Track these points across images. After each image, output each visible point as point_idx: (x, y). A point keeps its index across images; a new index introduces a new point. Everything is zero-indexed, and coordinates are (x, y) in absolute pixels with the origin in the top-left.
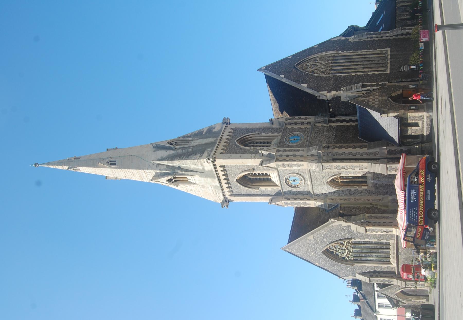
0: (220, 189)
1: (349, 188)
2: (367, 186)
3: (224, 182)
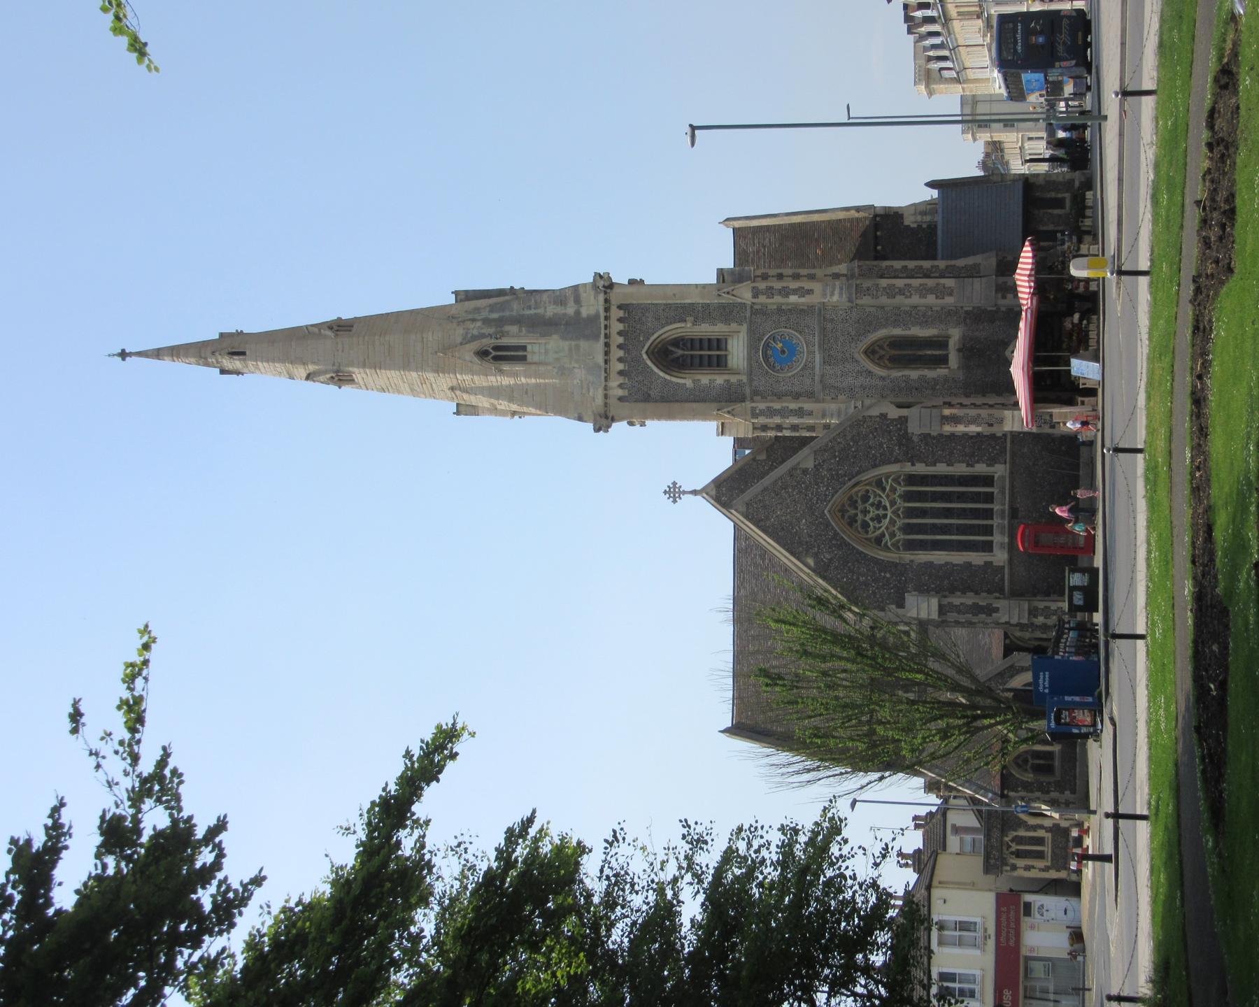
0: (603, 374)
1: (906, 372)
2: (949, 368)
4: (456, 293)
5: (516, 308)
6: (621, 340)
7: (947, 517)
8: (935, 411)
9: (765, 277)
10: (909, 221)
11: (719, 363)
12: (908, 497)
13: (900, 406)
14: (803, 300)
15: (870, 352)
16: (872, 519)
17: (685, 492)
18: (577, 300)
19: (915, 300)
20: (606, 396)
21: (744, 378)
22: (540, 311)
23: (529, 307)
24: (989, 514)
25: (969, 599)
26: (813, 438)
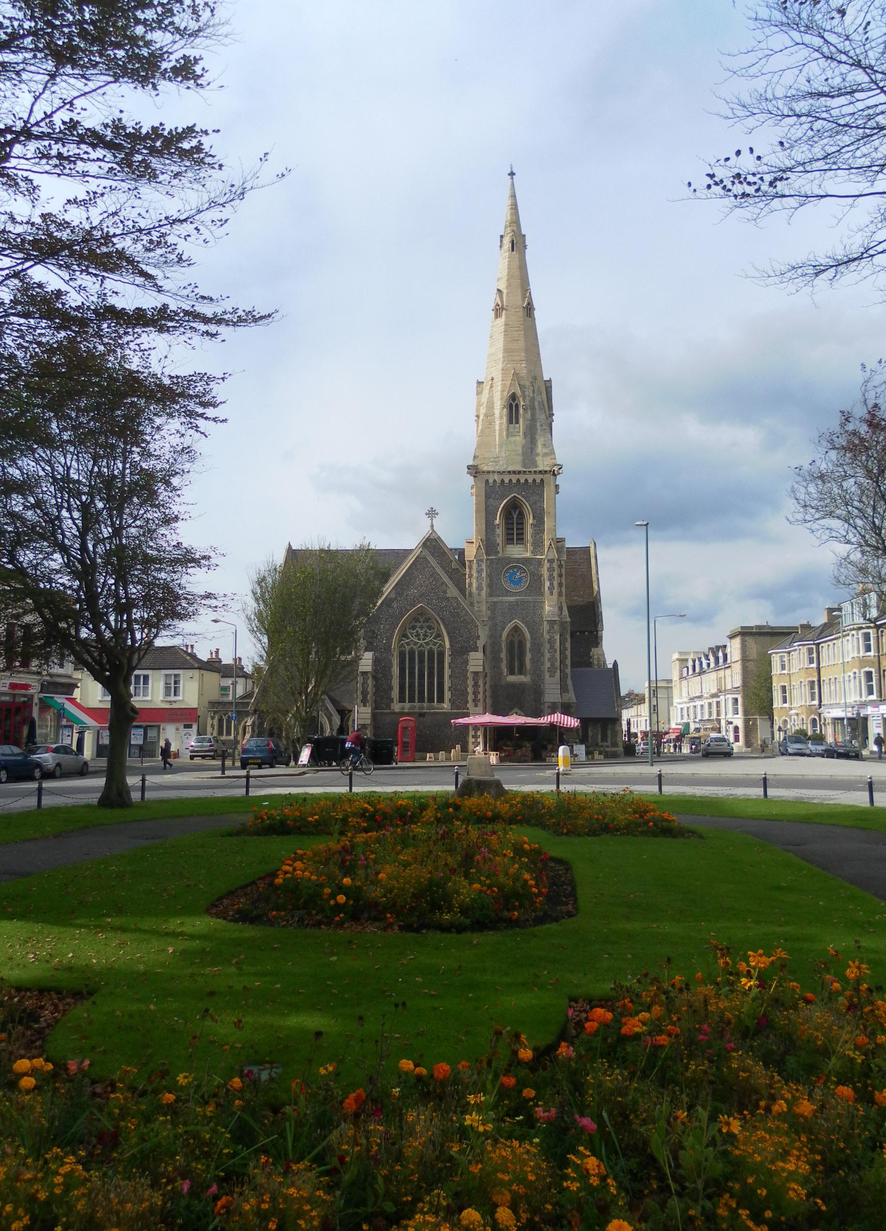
1: (504, 650)
3: (514, 478)
4: (550, 381)
5: (541, 417)
6: (522, 481)
7: (419, 676)
8: (480, 669)
9: (560, 566)
10: (594, 651)
11: (509, 540)
12: (431, 653)
13: (484, 647)
14: (546, 589)
15: (516, 629)
16: (417, 632)
17: (432, 520)
18: (545, 455)
19: (547, 655)
20: (489, 472)
21: (500, 555)
22: (539, 431)
23: (541, 426)
24: (421, 700)
25: (370, 689)
26: (464, 595)
